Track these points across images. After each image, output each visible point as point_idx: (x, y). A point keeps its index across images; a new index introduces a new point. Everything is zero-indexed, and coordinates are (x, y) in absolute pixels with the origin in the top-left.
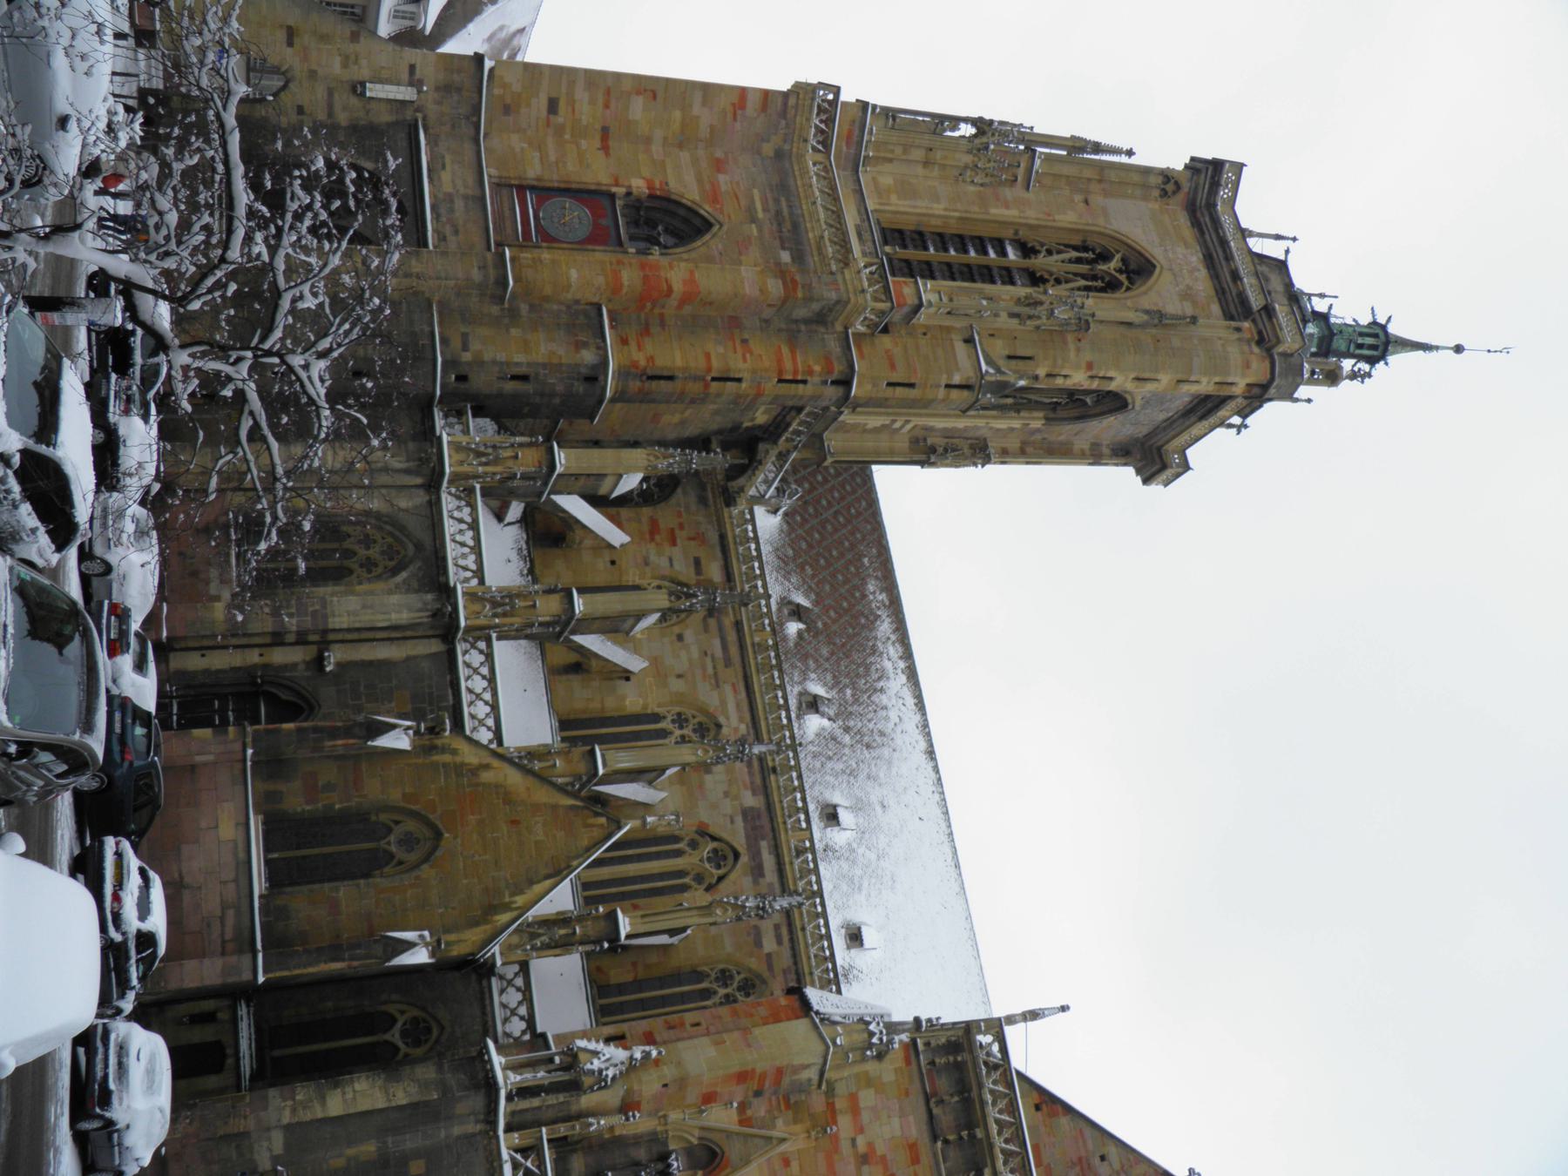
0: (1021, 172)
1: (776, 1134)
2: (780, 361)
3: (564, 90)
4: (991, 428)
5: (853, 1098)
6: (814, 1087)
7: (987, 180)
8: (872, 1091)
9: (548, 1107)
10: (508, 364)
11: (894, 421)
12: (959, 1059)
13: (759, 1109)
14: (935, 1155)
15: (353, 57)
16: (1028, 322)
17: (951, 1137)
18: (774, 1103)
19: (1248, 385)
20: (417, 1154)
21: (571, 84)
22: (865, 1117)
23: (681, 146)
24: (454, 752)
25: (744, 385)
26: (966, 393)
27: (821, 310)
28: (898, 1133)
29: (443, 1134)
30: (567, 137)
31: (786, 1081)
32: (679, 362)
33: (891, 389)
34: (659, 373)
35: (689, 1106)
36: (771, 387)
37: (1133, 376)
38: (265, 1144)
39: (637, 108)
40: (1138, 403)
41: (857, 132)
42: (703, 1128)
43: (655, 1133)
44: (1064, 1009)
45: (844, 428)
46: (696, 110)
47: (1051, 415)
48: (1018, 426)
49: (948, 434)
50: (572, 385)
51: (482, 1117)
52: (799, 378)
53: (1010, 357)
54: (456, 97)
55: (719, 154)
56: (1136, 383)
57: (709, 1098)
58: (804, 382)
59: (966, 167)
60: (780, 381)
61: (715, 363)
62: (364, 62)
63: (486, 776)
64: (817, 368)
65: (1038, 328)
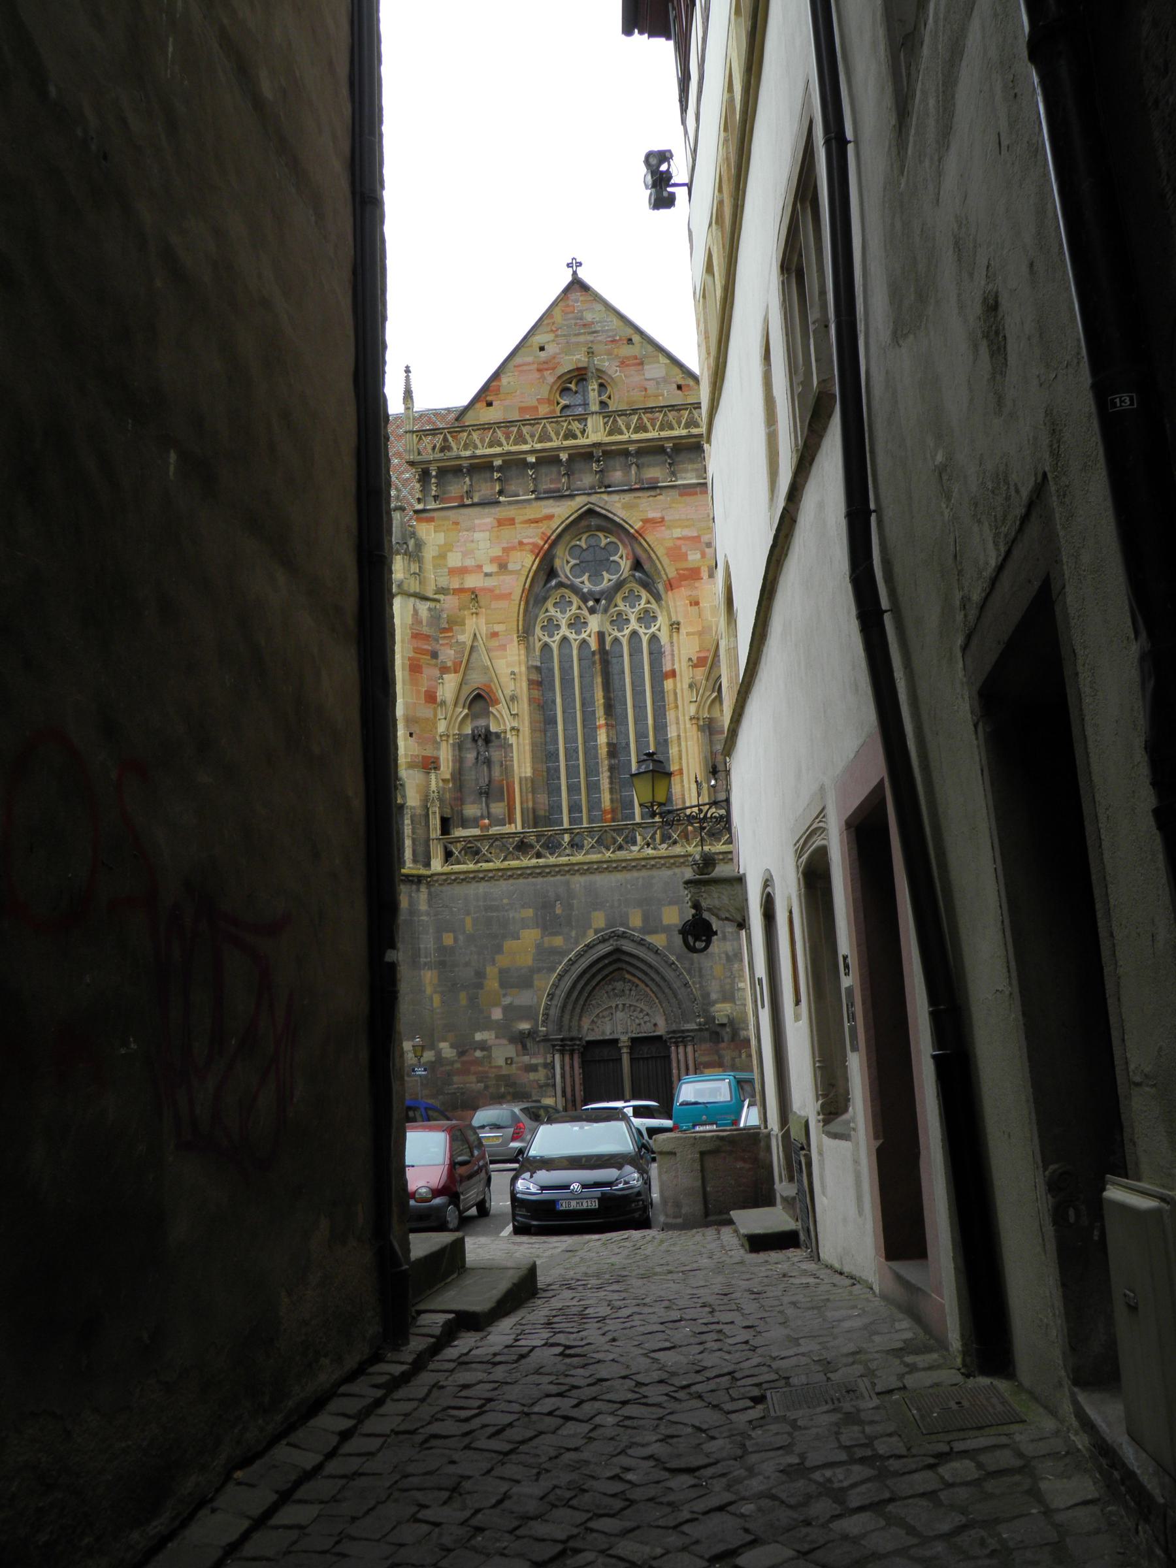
1: (469, 643)
5: (453, 572)
8: (449, 554)
9: (413, 833)
12: (434, 473)
13: (448, 655)
14: (510, 503)
17: (497, 489)
18: (446, 641)
20: (439, 939)
22: (469, 562)
28: (488, 533)
29: (424, 918)
31: (425, 630)
35: (435, 715)
42: (456, 705)
43: (453, 745)
44: (408, 370)
51: (414, 887)
57: (431, 697)
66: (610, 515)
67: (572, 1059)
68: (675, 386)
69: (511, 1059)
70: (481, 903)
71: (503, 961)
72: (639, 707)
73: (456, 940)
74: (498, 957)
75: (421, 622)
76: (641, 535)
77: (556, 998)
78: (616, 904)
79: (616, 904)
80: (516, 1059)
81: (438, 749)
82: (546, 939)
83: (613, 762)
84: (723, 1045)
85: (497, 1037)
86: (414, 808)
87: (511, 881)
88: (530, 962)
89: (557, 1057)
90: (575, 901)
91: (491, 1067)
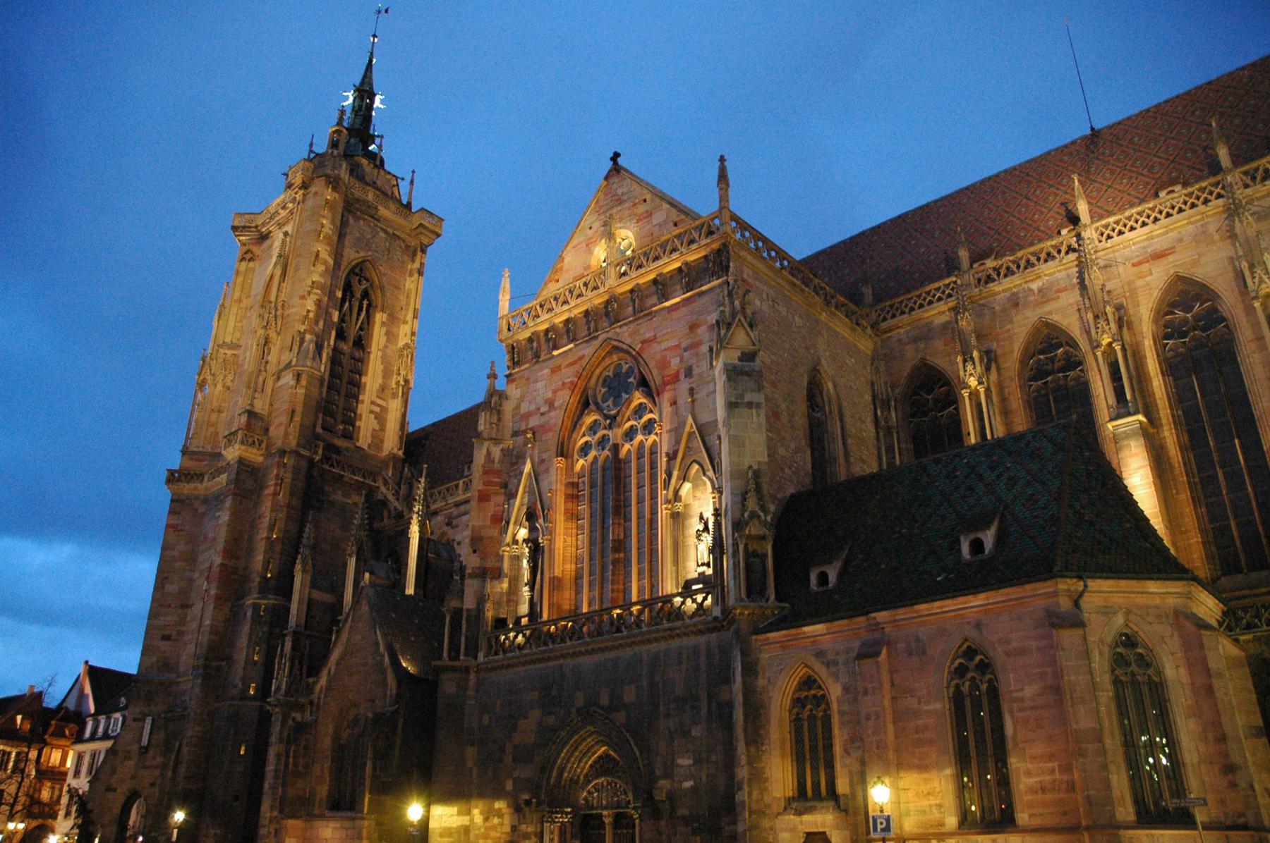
0: (229, 352)
2: (269, 495)
4: (386, 346)
9: (467, 631)
11: (371, 412)
23: (195, 560)
24: (321, 691)
30: (184, 628)
31: (497, 466)
38: (444, 818)
39: (171, 588)
40: (362, 254)
45: (378, 439)
46: (176, 553)
47: (379, 308)
48: (384, 330)
55: (202, 538)
62: (129, 748)
63: (332, 671)
68: (672, 224)
72: (640, 501)
75: (493, 461)
76: (639, 355)
84: (663, 823)
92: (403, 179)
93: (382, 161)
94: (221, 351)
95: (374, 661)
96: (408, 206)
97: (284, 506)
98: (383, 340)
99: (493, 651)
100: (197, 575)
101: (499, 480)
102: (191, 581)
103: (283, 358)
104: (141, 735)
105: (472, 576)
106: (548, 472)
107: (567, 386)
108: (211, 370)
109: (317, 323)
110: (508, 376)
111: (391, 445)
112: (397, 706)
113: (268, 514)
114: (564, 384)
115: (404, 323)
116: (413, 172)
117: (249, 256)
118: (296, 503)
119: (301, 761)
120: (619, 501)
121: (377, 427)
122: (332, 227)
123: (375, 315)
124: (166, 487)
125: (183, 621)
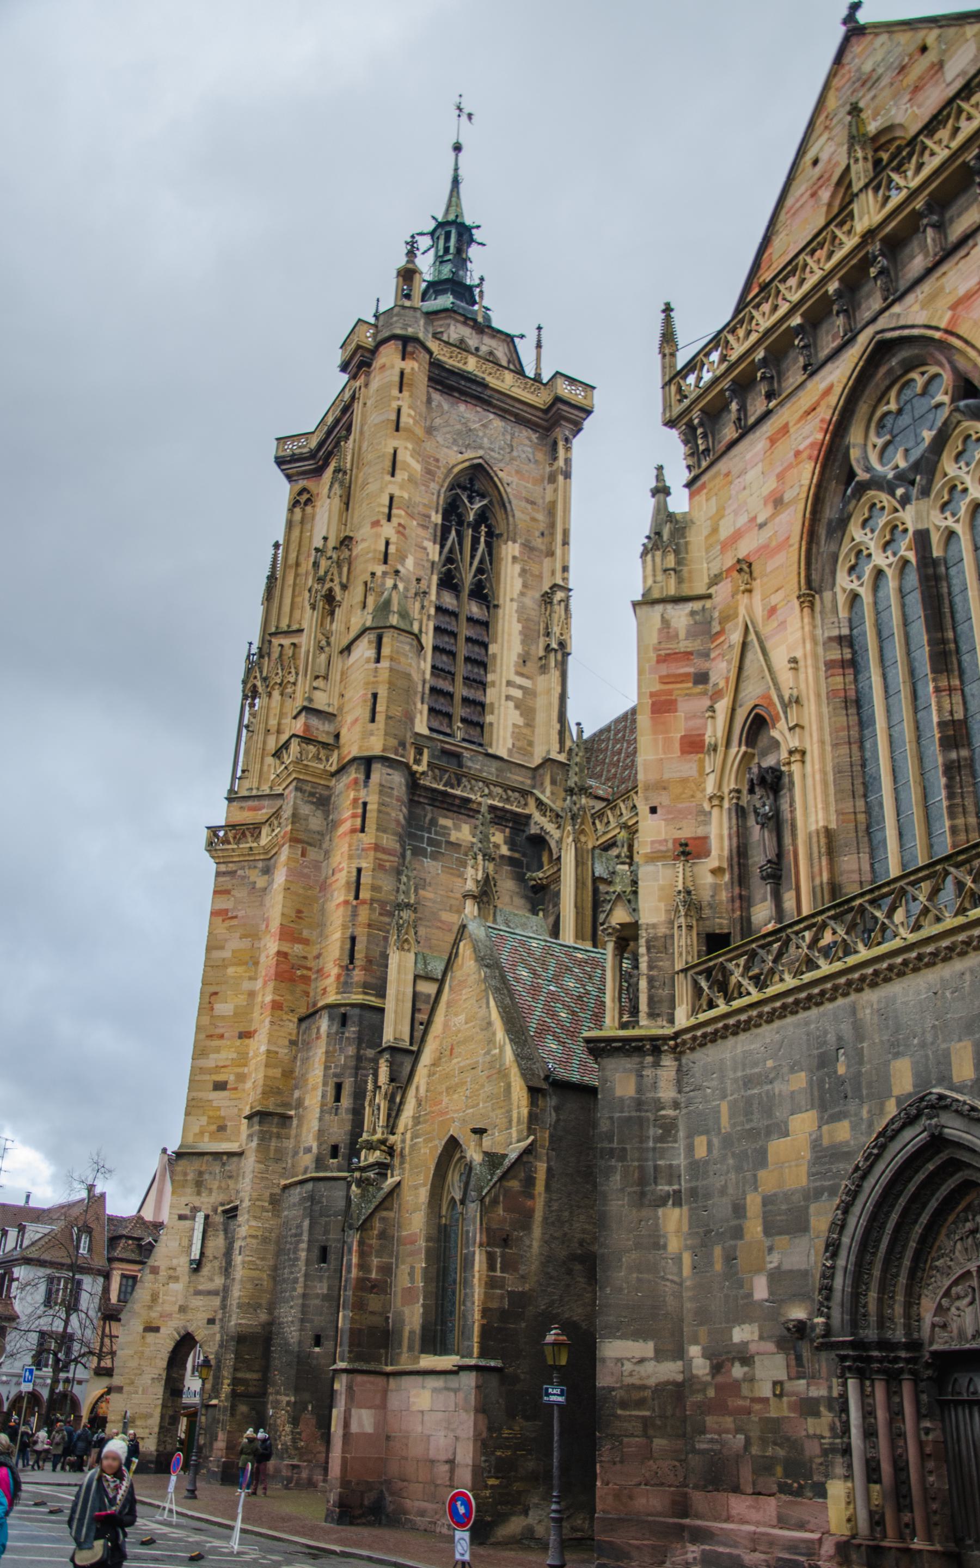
0: (286, 642)
2: (345, 834)
3: (207, 1077)
4: (522, 594)
6: (708, 604)
7: (293, 670)
9: (650, 967)
10: (323, 1105)
11: (508, 698)
14: (780, 404)
15: (171, 1272)
16: (338, 598)
19: (403, 359)
21: (202, 1070)
24: (406, 1126)
25: (364, 865)
26: (385, 640)
27: (313, 803)
31: (684, 645)
32: (338, 935)
33: (378, 717)
34: (347, 953)
36: (368, 838)
37: (388, 478)
38: (628, 1366)
40: (469, 454)
41: (250, 803)
46: (226, 954)
47: (505, 535)
48: (517, 568)
49: (527, 637)
50: (348, 1038)
51: (649, 1059)
52: (360, 811)
53: (364, 607)
54: (206, 1176)
56: (397, 472)
58: (365, 804)
59: (282, 694)
60: (363, 830)
61: (342, 899)
62: (175, 1262)
64: (352, 796)
65: (344, 587)
66: (906, 332)
67: (893, 1392)
69: (781, 1383)
70: (739, 1074)
71: (768, 1180)
73: (710, 1145)
74: (762, 1174)
75: (677, 635)
77: (843, 1253)
78: (929, 1038)
79: (929, 1038)
80: (788, 1386)
81: (707, 823)
82: (825, 1128)
83: (953, 755)
85: (761, 1338)
86: (654, 926)
87: (777, 1024)
88: (804, 1181)
89: (852, 1383)
90: (865, 1045)
91: (754, 1400)
92: (522, 337)
93: (487, 319)
94: (276, 641)
95: (488, 1058)
96: (537, 379)
97: (369, 849)
98: (518, 584)
99: (704, 1002)
100: (259, 984)
101: (691, 670)
102: (252, 994)
103: (353, 620)
104: (191, 1241)
105: (652, 858)
106: (785, 628)
107: (805, 455)
108: (261, 672)
109: (402, 558)
110: (689, 485)
111: (545, 748)
112: (532, 1138)
113: (344, 865)
114: (798, 454)
115: (547, 556)
116: (539, 328)
117: (305, 497)
118: (389, 841)
119: (375, 1261)
120: (944, 641)
121: (520, 722)
122: (412, 413)
123: (499, 546)
124: (207, 854)
125: (243, 1059)
